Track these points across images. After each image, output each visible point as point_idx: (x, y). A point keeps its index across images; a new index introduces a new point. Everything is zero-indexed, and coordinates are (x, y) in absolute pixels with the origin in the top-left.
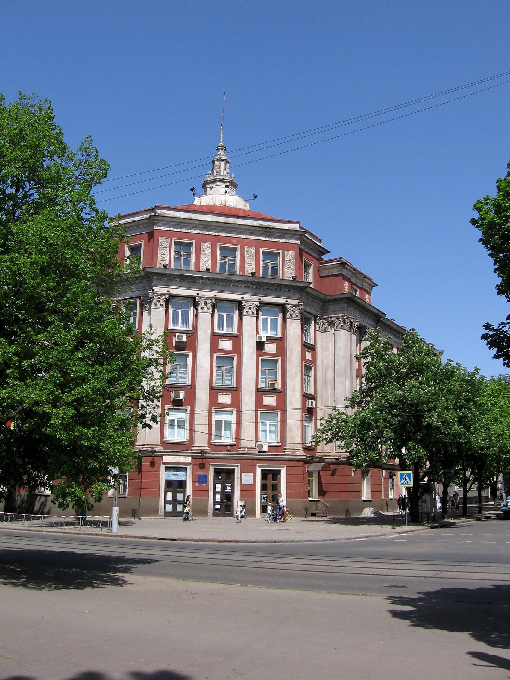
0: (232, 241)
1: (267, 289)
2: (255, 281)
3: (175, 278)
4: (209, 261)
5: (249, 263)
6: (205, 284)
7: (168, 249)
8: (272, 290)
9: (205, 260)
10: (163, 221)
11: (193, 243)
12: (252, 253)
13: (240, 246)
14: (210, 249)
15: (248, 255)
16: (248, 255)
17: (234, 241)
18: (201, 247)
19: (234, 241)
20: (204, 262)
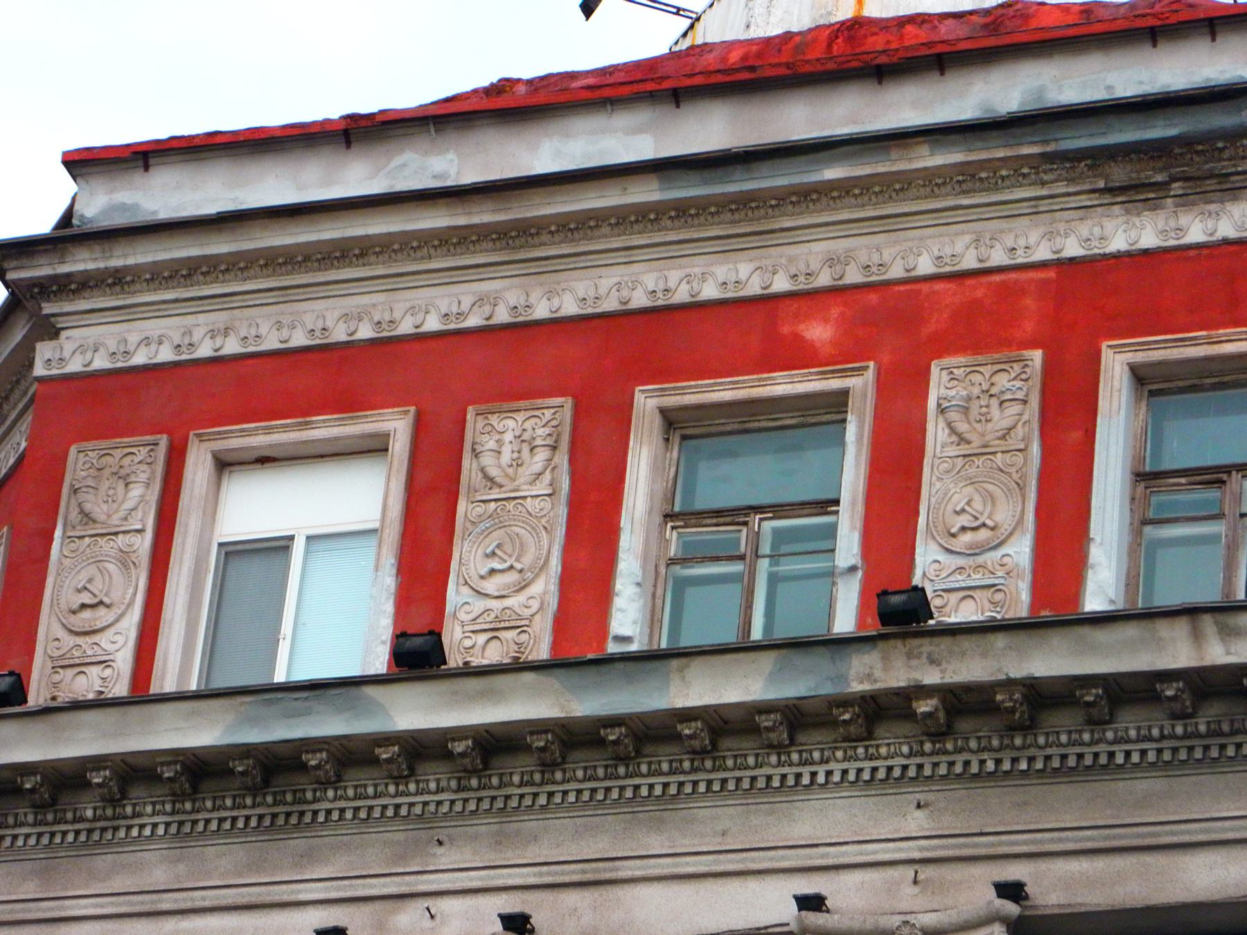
0: (797, 337)
1: (1108, 769)
2: (922, 691)
3: (114, 799)
4: (537, 588)
5: (964, 520)
6: (424, 819)
7: (144, 544)
8: (1162, 767)
9: (491, 586)
10: (118, 280)
11: (387, 436)
12: (1001, 418)
13: (870, 374)
14: (562, 459)
15: (962, 440)
16: (962, 440)
17: (819, 332)
18: (467, 463)
19: (819, 332)
20: (479, 605)
